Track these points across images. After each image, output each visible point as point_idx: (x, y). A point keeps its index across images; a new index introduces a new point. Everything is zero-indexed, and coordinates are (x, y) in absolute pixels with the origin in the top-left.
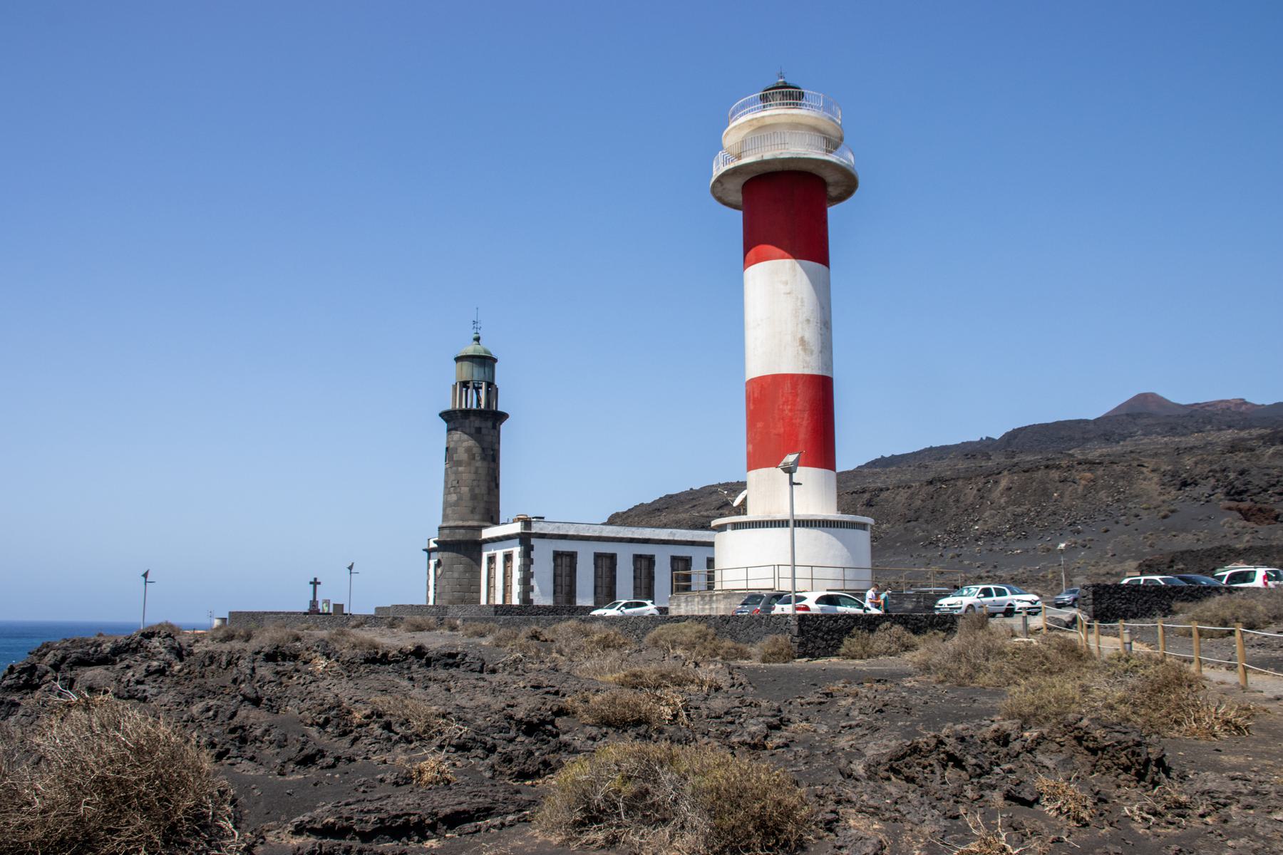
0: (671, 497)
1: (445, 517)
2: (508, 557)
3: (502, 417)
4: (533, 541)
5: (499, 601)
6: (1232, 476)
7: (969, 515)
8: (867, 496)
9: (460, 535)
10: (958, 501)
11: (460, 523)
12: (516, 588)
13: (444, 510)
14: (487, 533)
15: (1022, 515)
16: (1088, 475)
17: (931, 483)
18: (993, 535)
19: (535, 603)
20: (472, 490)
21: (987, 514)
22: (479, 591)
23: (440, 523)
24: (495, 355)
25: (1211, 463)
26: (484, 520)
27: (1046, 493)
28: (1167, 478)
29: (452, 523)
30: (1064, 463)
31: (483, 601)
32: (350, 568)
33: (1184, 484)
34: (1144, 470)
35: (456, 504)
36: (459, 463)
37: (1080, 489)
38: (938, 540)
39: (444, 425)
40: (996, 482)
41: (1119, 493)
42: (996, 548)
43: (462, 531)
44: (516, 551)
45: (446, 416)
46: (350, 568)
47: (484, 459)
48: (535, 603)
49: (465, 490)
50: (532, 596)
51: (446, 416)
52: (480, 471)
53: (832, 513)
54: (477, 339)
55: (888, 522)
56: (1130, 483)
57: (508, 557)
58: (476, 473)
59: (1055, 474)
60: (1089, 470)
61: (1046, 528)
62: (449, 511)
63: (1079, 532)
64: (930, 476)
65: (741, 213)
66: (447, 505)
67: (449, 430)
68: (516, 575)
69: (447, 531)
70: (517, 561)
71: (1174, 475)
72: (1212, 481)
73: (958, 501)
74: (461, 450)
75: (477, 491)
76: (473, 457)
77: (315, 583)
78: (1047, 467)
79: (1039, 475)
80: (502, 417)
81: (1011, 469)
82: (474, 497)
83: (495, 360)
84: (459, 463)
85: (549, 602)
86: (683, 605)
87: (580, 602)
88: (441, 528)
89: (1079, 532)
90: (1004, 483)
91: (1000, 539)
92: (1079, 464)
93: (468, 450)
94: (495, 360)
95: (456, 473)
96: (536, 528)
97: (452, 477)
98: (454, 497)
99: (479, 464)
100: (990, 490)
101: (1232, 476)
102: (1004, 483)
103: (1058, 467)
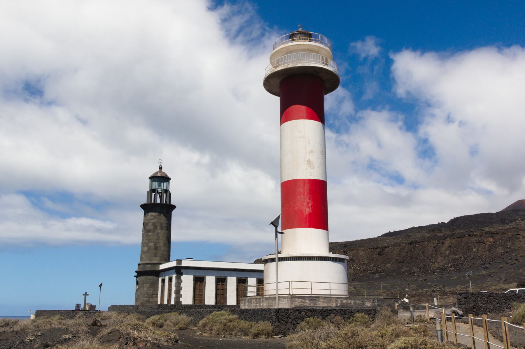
1: (142, 259)
2: (170, 280)
3: (174, 207)
4: (183, 271)
5: (166, 302)
7: (430, 260)
8: (378, 250)
9: (148, 268)
10: (423, 252)
11: (149, 262)
12: (173, 296)
13: (141, 255)
14: (162, 267)
15: (458, 259)
16: (491, 240)
17: (410, 243)
18: (443, 270)
19: (183, 304)
20: (155, 244)
21: (439, 259)
22: (157, 297)
23: (139, 262)
24: (169, 177)
26: (161, 260)
27: (469, 249)
29: (144, 262)
30: (478, 233)
31: (159, 303)
32: (101, 286)
34: (520, 236)
35: (147, 252)
36: (149, 231)
37: (487, 246)
38: (414, 272)
39: (142, 212)
40: (443, 243)
41: (507, 248)
43: (149, 266)
44: (174, 276)
45: (143, 206)
46: (101, 286)
47: (162, 228)
48: (183, 304)
49: (152, 244)
50: (181, 299)
51: (143, 206)
52: (160, 235)
53: (325, 253)
54: (161, 168)
55: (389, 263)
58: (158, 235)
59: (474, 239)
60: (491, 237)
62: (143, 256)
63: (487, 268)
64: (410, 241)
65: (279, 98)
66: (143, 252)
67: (145, 214)
68: (174, 288)
69: (141, 266)
70: (174, 281)
73: (423, 252)
74: (150, 224)
75: (158, 245)
76: (155, 227)
77: (86, 295)
78: (469, 235)
79: (465, 239)
80: (174, 207)
81: (451, 236)
82: (156, 248)
83: (170, 179)
84: (149, 231)
85: (213, 303)
86: (247, 303)
87: (207, 303)
88: (139, 265)
89: (487, 268)
91: (446, 272)
92: (486, 234)
94: (170, 179)
95: (147, 236)
96: (184, 264)
97: (145, 238)
98: (146, 248)
99: (159, 231)
100: (440, 247)
103: (475, 236)
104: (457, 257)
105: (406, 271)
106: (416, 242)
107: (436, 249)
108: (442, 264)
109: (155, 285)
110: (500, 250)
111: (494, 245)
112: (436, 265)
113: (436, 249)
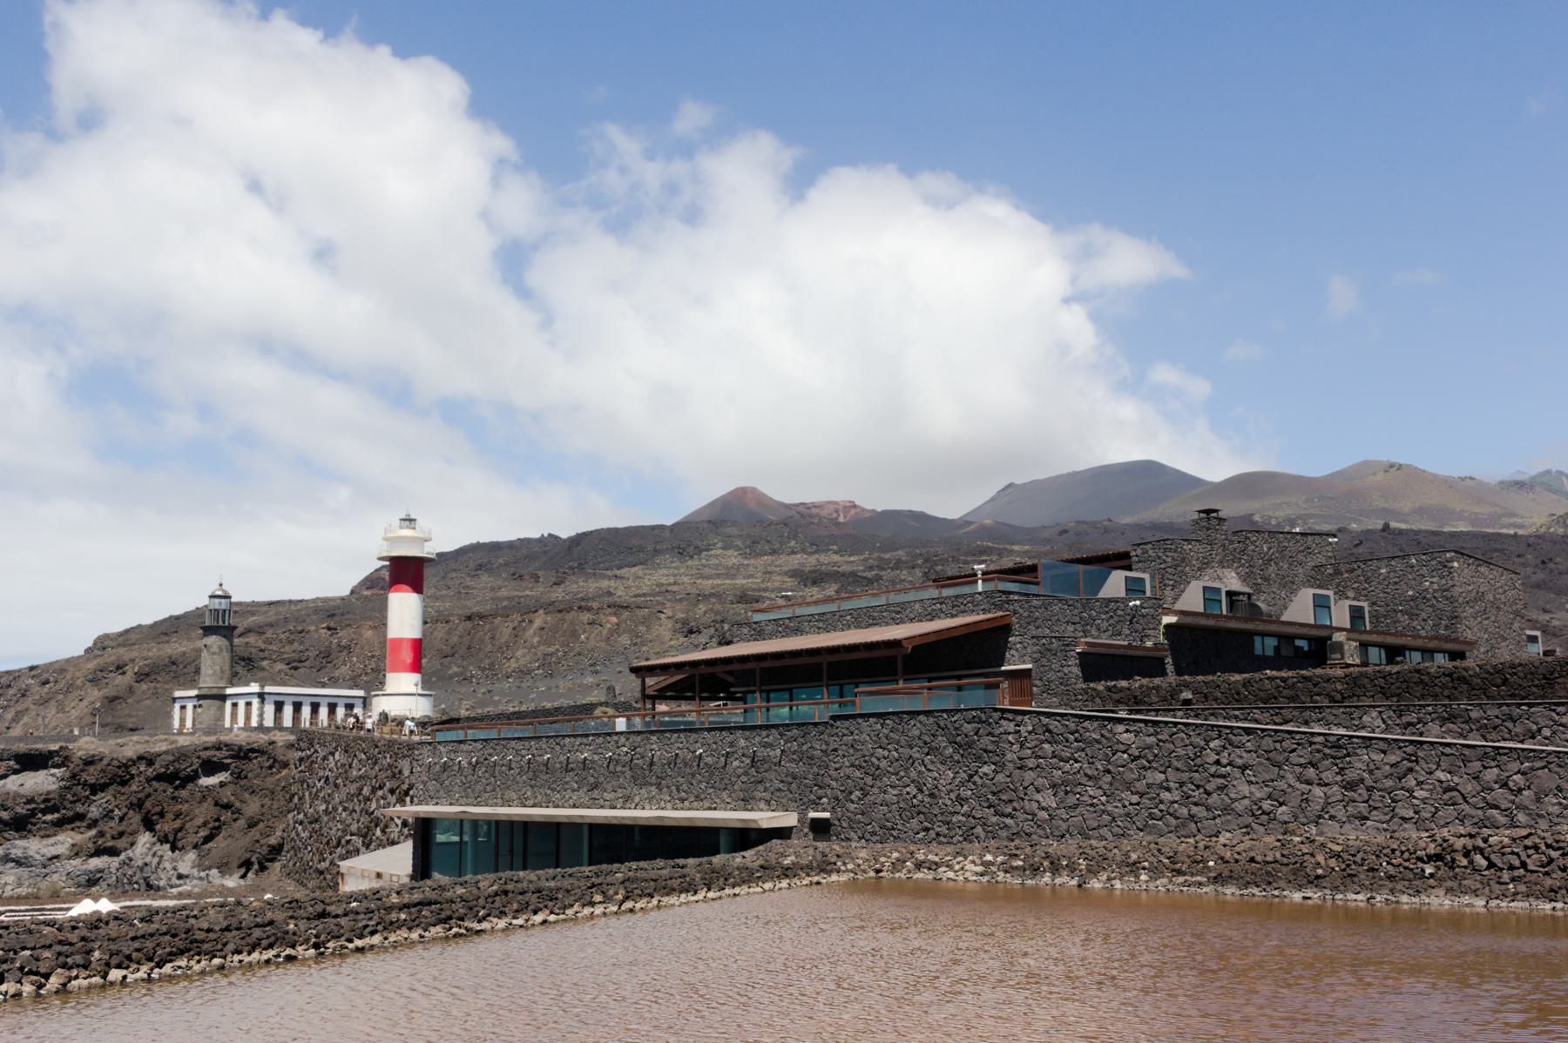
0: (177, 618)
2: (249, 704)
6: (726, 627)
9: (215, 691)
10: (493, 638)
15: (551, 654)
16: (614, 619)
17: (469, 618)
18: (523, 673)
21: (519, 653)
25: (717, 613)
27: (574, 635)
28: (678, 626)
30: (595, 605)
33: (691, 632)
35: (214, 674)
42: (524, 685)
56: (649, 628)
57: (249, 704)
59: (586, 617)
61: (570, 669)
64: (468, 612)
71: (685, 623)
72: (712, 630)
73: (493, 638)
81: (549, 607)
90: (538, 622)
93: (220, 648)
101: (726, 627)
102: (538, 622)
103: (589, 609)
104: (551, 650)
105: (456, 674)
106: (482, 617)
107: (517, 632)
108: (523, 661)
109: (222, 709)
110: (625, 640)
111: (616, 630)
112: (513, 664)
113: (517, 632)
